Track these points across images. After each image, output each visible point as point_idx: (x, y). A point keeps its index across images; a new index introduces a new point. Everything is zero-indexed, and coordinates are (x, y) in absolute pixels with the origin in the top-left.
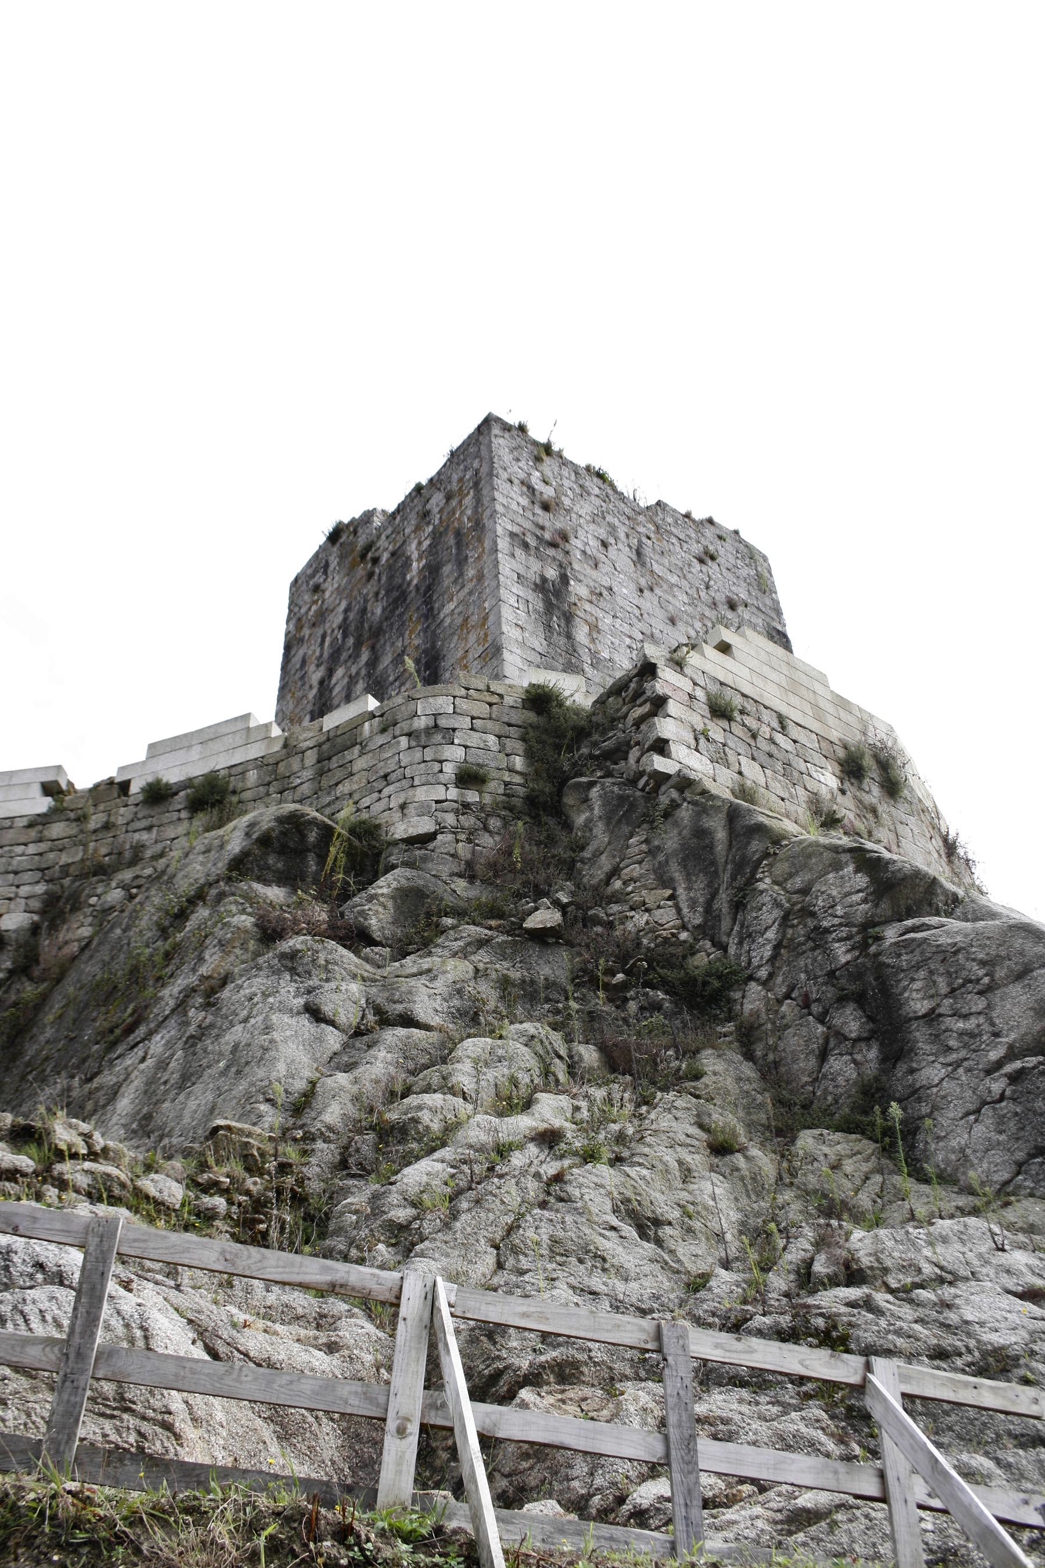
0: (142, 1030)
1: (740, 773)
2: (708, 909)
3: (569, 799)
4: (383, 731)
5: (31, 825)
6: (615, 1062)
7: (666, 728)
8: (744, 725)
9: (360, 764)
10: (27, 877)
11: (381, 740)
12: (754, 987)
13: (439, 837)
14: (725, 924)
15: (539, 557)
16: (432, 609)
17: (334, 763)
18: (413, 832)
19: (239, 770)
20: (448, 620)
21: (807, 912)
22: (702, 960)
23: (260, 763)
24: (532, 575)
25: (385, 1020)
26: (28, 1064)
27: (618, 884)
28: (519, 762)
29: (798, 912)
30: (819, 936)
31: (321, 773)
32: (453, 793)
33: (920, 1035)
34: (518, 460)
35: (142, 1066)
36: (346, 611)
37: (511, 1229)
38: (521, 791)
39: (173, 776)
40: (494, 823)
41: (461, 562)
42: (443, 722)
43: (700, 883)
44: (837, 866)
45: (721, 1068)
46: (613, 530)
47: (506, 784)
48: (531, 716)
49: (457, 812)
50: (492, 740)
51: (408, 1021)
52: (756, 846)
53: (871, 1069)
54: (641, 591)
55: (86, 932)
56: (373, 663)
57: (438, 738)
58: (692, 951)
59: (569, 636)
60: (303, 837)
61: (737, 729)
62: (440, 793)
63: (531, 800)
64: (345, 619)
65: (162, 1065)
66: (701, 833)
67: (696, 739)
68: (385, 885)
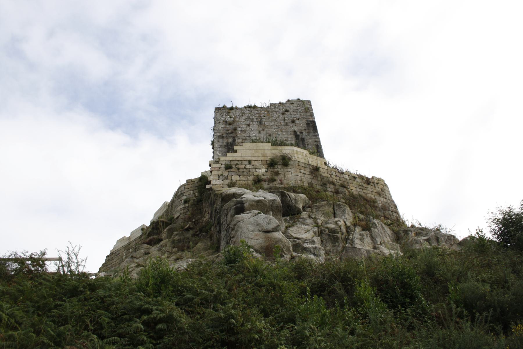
24: (224, 144)
62: (181, 207)
67: (219, 177)
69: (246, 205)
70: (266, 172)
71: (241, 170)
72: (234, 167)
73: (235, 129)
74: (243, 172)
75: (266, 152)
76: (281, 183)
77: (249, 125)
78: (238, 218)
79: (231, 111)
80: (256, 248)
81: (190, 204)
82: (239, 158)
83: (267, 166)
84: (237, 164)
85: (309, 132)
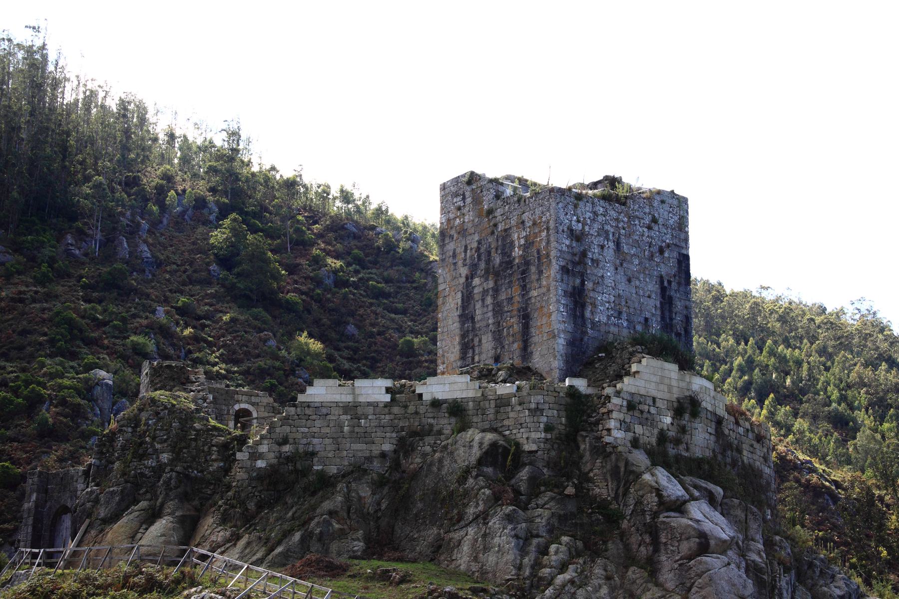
0: (462, 523)
2: (616, 493)
3: (579, 439)
4: (520, 404)
5: (385, 406)
6: (587, 546)
7: (612, 424)
9: (512, 415)
10: (388, 429)
11: (518, 408)
12: (626, 521)
14: (621, 498)
15: (574, 275)
16: (525, 286)
17: (502, 410)
18: (530, 449)
19: (467, 400)
20: (533, 301)
21: (641, 503)
22: (614, 506)
23: (474, 399)
24: (570, 289)
26: (416, 515)
27: (591, 475)
29: (639, 503)
30: (643, 512)
31: (497, 412)
32: (543, 435)
33: (662, 547)
34: (567, 214)
35: (468, 537)
36: (479, 242)
38: (563, 432)
39: (440, 396)
40: (556, 446)
41: (540, 272)
42: (540, 407)
43: (615, 484)
44: (652, 493)
45: (613, 547)
48: (568, 400)
49: (545, 443)
51: (538, 536)
52: (631, 477)
53: (650, 552)
54: (617, 269)
55: (418, 460)
56: (496, 290)
58: (611, 504)
61: (637, 414)
62: (538, 435)
64: (478, 249)
65: (476, 540)
68: (524, 474)
69: (712, 542)
71: (645, 415)
73: (584, 254)
76: (687, 450)
77: (602, 247)
78: (706, 563)
79: (581, 204)
82: (642, 392)
84: (640, 403)
85: (679, 284)
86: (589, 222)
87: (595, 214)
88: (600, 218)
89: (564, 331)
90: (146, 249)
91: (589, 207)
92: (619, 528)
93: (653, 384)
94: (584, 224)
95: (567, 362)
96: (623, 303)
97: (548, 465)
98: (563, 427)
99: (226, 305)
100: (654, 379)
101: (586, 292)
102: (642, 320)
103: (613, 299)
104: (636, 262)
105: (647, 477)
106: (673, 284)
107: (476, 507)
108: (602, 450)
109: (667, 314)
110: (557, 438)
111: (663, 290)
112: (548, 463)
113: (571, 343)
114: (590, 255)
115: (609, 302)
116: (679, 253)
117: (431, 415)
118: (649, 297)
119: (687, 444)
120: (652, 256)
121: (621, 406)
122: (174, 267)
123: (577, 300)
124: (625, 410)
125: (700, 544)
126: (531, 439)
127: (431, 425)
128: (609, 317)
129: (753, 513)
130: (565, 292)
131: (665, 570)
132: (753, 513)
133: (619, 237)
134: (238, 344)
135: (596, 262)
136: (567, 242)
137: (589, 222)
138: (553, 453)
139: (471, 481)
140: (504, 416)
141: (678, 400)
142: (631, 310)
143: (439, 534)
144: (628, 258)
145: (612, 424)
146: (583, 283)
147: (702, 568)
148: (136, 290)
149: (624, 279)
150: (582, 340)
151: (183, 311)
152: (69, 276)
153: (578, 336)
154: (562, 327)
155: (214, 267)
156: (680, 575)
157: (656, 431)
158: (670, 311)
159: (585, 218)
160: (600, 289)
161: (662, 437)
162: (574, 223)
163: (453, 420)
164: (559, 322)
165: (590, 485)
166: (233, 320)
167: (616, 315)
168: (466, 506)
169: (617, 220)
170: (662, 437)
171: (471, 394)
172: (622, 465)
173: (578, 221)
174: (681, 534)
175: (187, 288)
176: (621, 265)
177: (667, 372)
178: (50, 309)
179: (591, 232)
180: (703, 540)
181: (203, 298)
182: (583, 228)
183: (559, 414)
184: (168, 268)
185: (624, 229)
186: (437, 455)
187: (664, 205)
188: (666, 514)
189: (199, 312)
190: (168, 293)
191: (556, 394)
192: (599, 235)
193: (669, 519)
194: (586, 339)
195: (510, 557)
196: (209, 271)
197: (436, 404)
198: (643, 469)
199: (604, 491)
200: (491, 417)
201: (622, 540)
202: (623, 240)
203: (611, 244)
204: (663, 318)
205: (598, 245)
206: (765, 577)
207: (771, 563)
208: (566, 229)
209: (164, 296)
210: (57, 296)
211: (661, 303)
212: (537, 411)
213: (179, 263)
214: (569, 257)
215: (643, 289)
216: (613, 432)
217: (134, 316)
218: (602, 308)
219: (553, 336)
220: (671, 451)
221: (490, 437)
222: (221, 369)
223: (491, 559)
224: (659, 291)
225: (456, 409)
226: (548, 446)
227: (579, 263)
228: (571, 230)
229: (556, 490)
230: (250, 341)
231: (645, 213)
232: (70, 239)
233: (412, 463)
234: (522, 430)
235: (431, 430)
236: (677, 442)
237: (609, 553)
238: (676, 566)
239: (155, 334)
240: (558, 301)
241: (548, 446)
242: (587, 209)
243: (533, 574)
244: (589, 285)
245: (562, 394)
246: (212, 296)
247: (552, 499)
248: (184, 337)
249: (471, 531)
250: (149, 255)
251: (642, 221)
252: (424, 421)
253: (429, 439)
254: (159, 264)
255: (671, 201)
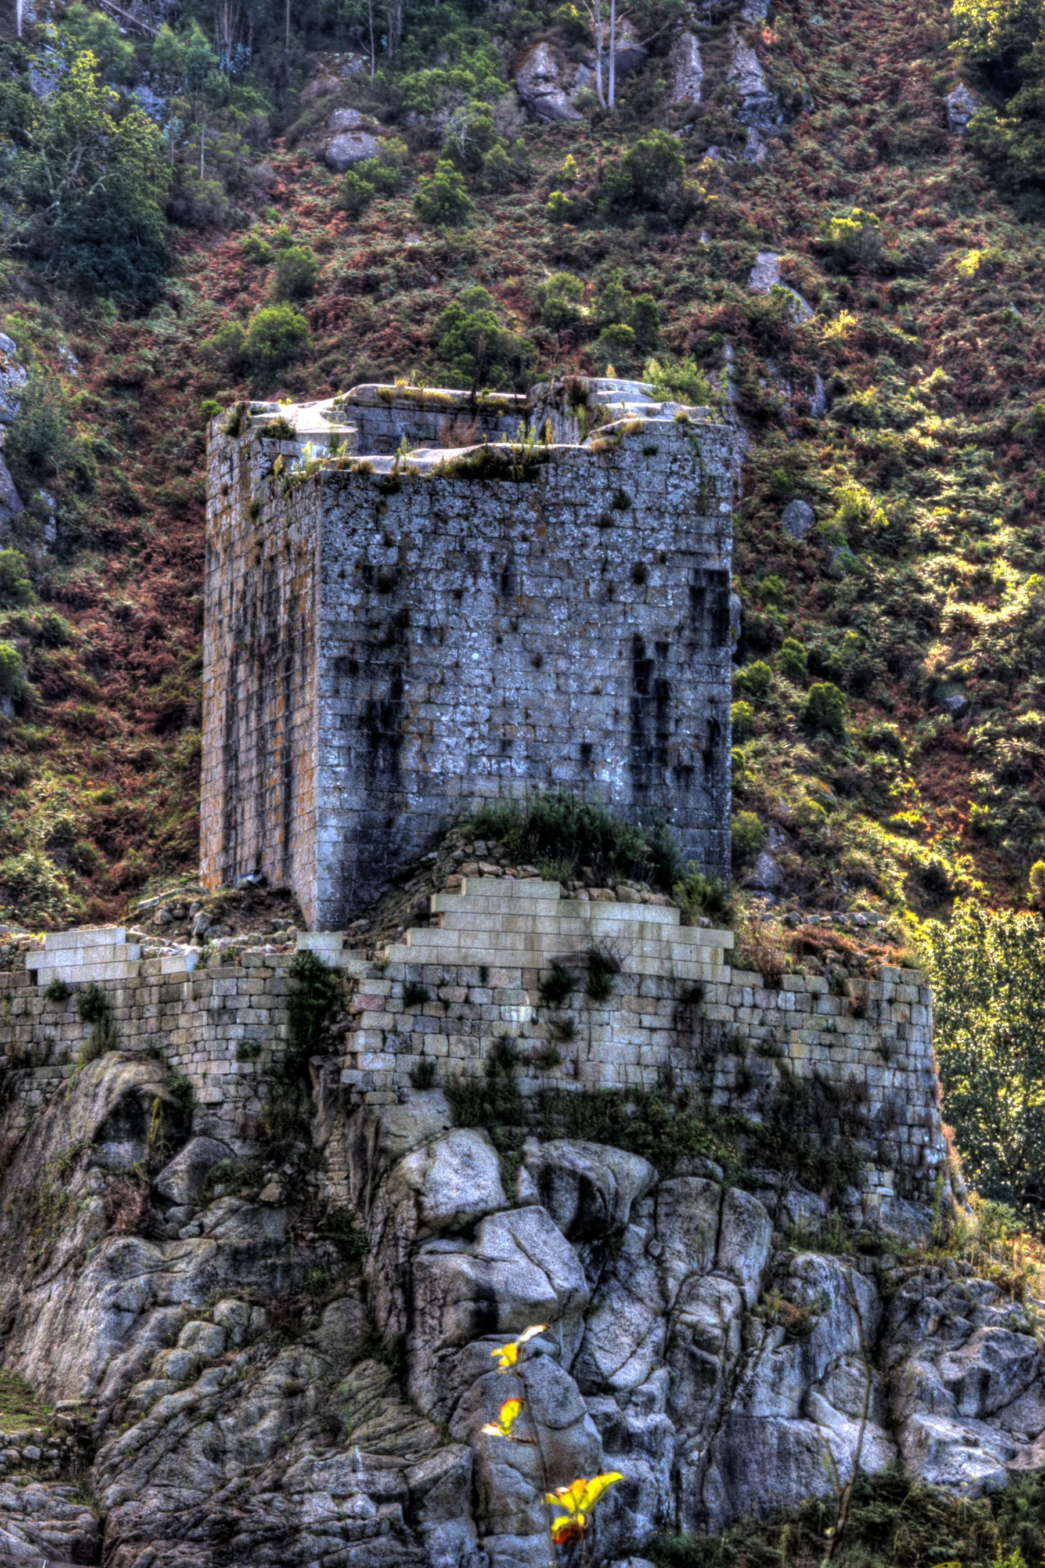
0: (48, 1273)
1: (422, 1053)
3: (312, 1072)
4: (195, 999)
8: (439, 999)
9: (183, 1021)
11: (192, 1007)
13: (226, 1106)
18: (209, 1099)
24: (359, 708)
25: (155, 1304)
28: (283, 1030)
31: (162, 1014)
32: (235, 1067)
33: (418, 1319)
37: (156, 1465)
40: (263, 1089)
42: (229, 1004)
46: (473, 559)
47: (273, 1052)
48: (295, 984)
49: (238, 1084)
50: (264, 1013)
51: (168, 1303)
54: (499, 640)
57: (225, 1018)
59: (394, 768)
60: (140, 1106)
63: (289, 1062)
66: (363, 1139)
67: (384, 1039)
69: (505, 1310)
70: (534, 1022)
71: (456, 1010)
72: (433, 995)
73: (402, 621)
74: (461, 1018)
75: (540, 928)
76: (576, 1075)
77: (459, 595)
78: (481, 1356)
79: (393, 501)
80: (526, 1469)
81: (259, 1068)
82: (451, 957)
83: (537, 995)
84: (443, 984)
85: (693, 646)
86: (419, 540)
87: (440, 517)
88: (453, 527)
89: (337, 812)
90: (753, 65)
91: (421, 503)
92: (360, 1272)
93: (485, 936)
94: (402, 551)
95: (345, 881)
96: (518, 718)
97: (242, 1134)
98: (282, 1046)
99: (982, 218)
100: (488, 924)
101: (407, 709)
102: (575, 755)
103: (484, 712)
104: (560, 613)
105: (412, 1162)
106: (673, 650)
107: (72, 1238)
108: (346, 1102)
109: (651, 725)
110: (265, 1073)
111: (641, 668)
112: (244, 1128)
113: (359, 835)
114: (420, 619)
115: (473, 724)
116: (697, 572)
117: (49, 1018)
118: (597, 692)
119: (575, 1062)
120: (611, 591)
121: (388, 998)
122: (838, 110)
123: (380, 734)
124: (397, 1004)
125: (476, 1314)
126: (212, 1074)
127: (51, 1042)
128: (471, 760)
129: (735, 1208)
130: (345, 718)
131: (419, 1368)
132: (735, 1208)
133: (511, 561)
134: (990, 347)
135: (436, 634)
136: (354, 600)
137: (419, 540)
138: (257, 1107)
139: (78, 1175)
140: (171, 1025)
141: (555, 965)
142: (542, 732)
143: (16, 1293)
144: (538, 608)
145: (359, 1041)
146: (397, 689)
147: (472, 1367)
148: (703, 207)
149: (520, 663)
150: (389, 823)
151: (840, 259)
152: (525, 181)
153: (380, 816)
154: (333, 801)
155: (959, 95)
156: (440, 1380)
157: (486, 1044)
158: (662, 717)
159: (406, 535)
160: (448, 695)
161: (504, 1056)
162: (372, 550)
163: (90, 1029)
164: (325, 791)
165: (321, 1175)
166: (990, 269)
167: (494, 750)
168: (60, 1231)
169: (506, 521)
170: (504, 1056)
171: (119, 972)
172: (370, 1133)
173: (388, 543)
174: (446, 1292)
175: (866, 179)
176: (515, 628)
177: (525, 904)
178: (438, 306)
179: (426, 563)
180: (484, 1305)
181: (913, 202)
182: (402, 557)
183: (271, 1017)
184: (817, 120)
185: (525, 539)
186: (50, 1111)
187: (652, 460)
188: (429, 1247)
189: (892, 255)
190: (807, 205)
191: (268, 973)
192: (449, 566)
193: (432, 1258)
194: (401, 820)
195: (89, 1355)
196: (944, 108)
197: (60, 993)
198: (411, 1140)
199: (342, 1191)
200: (153, 1023)
201: (364, 1300)
202: (522, 567)
203: (486, 584)
204: (637, 736)
205: (446, 592)
206: (717, 1360)
207: (745, 1325)
208: (349, 568)
209: (791, 214)
210: (471, 259)
211: (634, 703)
212: (223, 1014)
213: (856, 93)
214: (356, 635)
215: (580, 677)
216: (360, 1058)
217: (687, 294)
218: (451, 741)
219: (319, 824)
220: (527, 1082)
221: (130, 1073)
222: (924, 433)
223: (65, 1356)
224: (628, 674)
225: (94, 1006)
226: (245, 1091)
227: (387, 643)
228: (366, 569)
229: (245, 1191)
230: (1030, 334)
231: (593, 491)
232: (542, 61)
233: (10, 1128)
234: (197, 1057)
235: (50, 1052)
236: (548, 1060)
237: (320, 1334)
238: (435, 1360)
239: (737, 345)
240: (324, 743)
241: (245, 1091)
242: (416, 509)
243: (120, 1395)
244: (414, 691)
245: (280, 973)
246: (941, 194)
247: (233, 1211)
248: (832, 344)
249: (56, 1289)
250: (759, 86)
251: (582, 512)
252: (39, 1031)
253: (43, 1074)
254: (792, 108)
255: (675, 446)
